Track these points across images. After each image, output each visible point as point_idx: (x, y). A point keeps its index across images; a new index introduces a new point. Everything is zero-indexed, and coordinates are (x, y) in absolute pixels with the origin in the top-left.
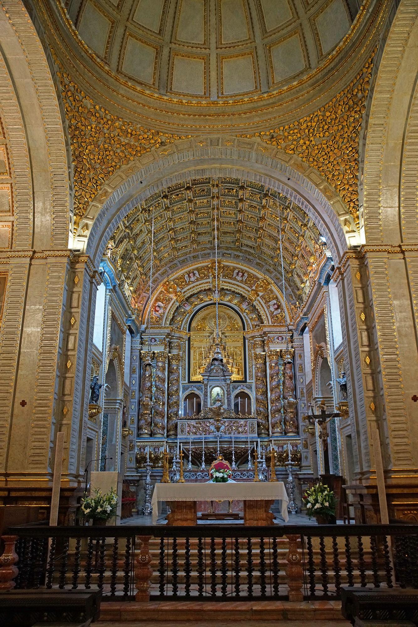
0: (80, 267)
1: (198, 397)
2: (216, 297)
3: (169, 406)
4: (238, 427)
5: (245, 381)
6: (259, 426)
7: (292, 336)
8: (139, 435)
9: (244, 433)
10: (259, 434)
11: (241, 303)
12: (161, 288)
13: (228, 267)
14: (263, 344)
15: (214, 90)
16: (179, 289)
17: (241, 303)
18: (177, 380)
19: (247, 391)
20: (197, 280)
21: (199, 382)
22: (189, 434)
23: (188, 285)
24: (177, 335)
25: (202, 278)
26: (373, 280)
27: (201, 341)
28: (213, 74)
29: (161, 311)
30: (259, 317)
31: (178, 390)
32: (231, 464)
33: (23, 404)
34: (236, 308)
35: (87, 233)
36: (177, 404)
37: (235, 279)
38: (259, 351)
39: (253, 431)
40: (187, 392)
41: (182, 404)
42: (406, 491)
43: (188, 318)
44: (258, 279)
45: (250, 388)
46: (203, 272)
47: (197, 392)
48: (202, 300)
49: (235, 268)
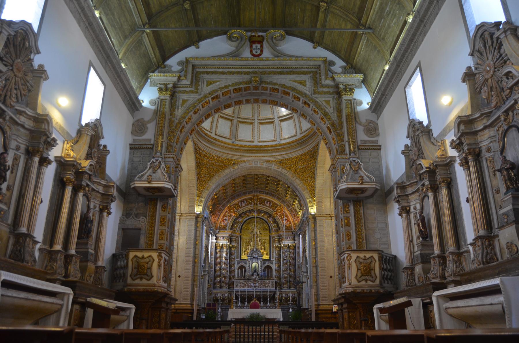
0: (200, 219)
1: (245, 268)
2: (255, 214)
3: (230, 272)
4: (265, 284)
5: (270, 260)
6: (276, 283)
7: (294, 237)
8: (214, 288)
9: (269, 288)
10: (276, 288)
11: (268, 217)
12: (226, 209)
13: (262, 198)
14: (280, 240)
15: (256, 137)
16: (236, 210)
17: (268, 217)
18: (234, 259)
19: (271, 265)
20: (246, 205)
21: (245, 260)
22: (240, 287)
23: (241, 208)
24: (235, 235)
25: (248, 204)
26: (318, 229)
27: (247, 236)
28: (256, 130)
29: (226, 222)
30: (278, 226)
31: (234, 264)
32: (260, 303)
33: (179, 276)
34: (266, 220)
35: (202, 204)
36: (234, 271)
37: (265, 205)
38: (277, 244)
39: (273, 286)
40: (239, 265)
41: (236, 271)
42: (324, 312)
43: (239, 225)
44: (278, 205)
45: (272, 263)
46: (248, 201)
47: (245, 265)
48: (248, 215)
49: (266, 199)
